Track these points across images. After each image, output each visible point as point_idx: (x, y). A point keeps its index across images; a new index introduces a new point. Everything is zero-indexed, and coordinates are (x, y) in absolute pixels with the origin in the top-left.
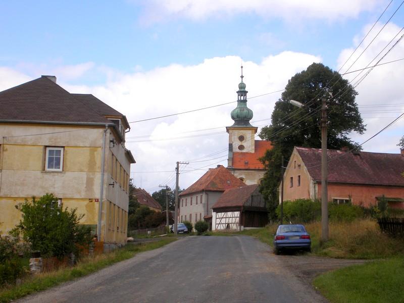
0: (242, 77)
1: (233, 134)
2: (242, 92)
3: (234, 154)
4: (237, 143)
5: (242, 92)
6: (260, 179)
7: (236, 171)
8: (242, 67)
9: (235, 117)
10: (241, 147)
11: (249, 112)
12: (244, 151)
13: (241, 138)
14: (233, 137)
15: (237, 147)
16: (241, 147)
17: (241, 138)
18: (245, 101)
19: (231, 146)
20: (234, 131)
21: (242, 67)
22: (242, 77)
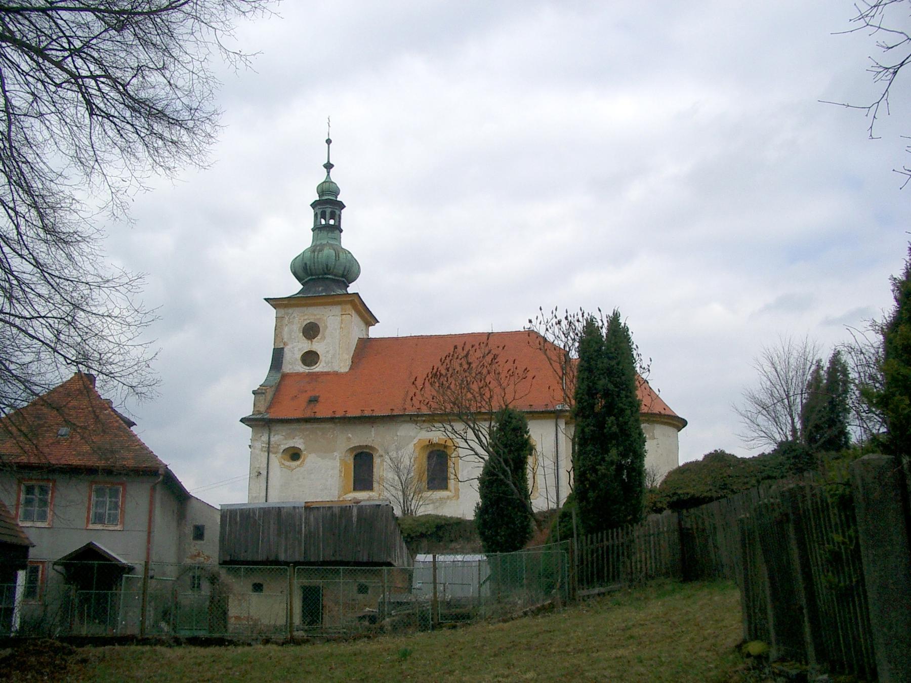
0: (329, 166)
1: (286, 321)
2: (328, 206)
3: (284, 376)
4: (297, 347)
5: (328, 206)
6: (352, 450)
7: (279, 427)
8: (329, 142)
9: (301, 273)
10: (310, 358)
11: (337, 256)
12: (317, 368)
13: (311, 331)
14: (286, 329)
15: (298, 356)
16: (310, 358)
17: (311, 331)
18: (337, 228)
19: (278, 356)
20: (290, 311)
21: (329, 142)
22: (329, 166)
